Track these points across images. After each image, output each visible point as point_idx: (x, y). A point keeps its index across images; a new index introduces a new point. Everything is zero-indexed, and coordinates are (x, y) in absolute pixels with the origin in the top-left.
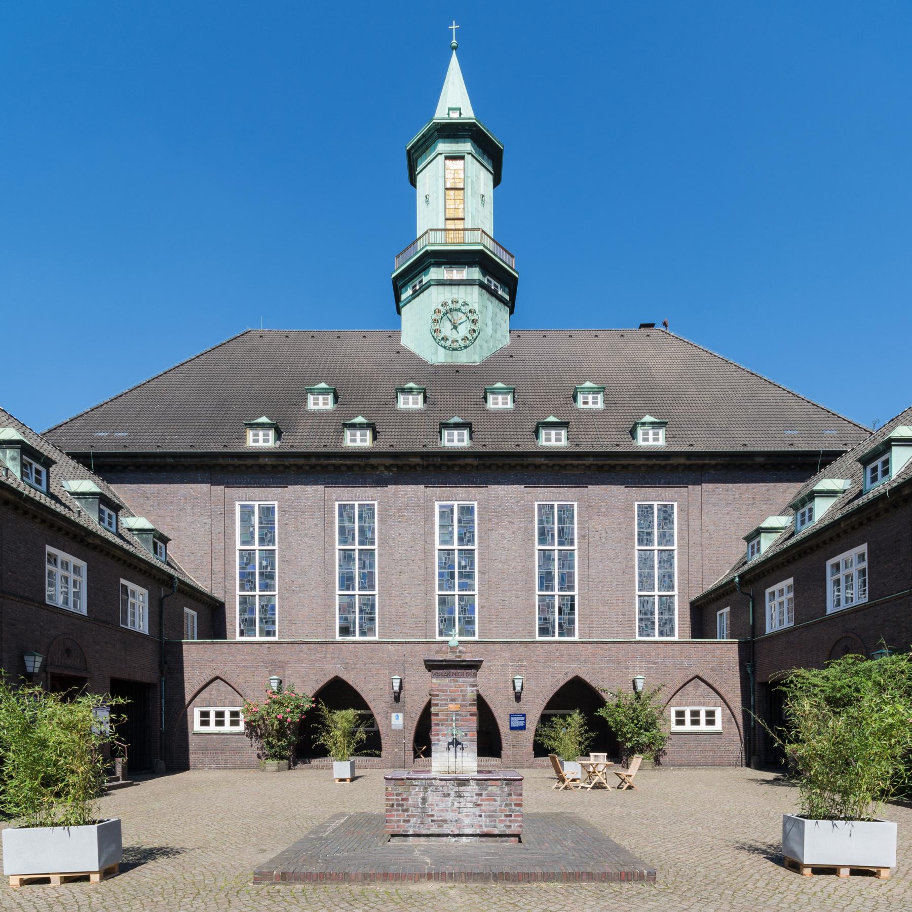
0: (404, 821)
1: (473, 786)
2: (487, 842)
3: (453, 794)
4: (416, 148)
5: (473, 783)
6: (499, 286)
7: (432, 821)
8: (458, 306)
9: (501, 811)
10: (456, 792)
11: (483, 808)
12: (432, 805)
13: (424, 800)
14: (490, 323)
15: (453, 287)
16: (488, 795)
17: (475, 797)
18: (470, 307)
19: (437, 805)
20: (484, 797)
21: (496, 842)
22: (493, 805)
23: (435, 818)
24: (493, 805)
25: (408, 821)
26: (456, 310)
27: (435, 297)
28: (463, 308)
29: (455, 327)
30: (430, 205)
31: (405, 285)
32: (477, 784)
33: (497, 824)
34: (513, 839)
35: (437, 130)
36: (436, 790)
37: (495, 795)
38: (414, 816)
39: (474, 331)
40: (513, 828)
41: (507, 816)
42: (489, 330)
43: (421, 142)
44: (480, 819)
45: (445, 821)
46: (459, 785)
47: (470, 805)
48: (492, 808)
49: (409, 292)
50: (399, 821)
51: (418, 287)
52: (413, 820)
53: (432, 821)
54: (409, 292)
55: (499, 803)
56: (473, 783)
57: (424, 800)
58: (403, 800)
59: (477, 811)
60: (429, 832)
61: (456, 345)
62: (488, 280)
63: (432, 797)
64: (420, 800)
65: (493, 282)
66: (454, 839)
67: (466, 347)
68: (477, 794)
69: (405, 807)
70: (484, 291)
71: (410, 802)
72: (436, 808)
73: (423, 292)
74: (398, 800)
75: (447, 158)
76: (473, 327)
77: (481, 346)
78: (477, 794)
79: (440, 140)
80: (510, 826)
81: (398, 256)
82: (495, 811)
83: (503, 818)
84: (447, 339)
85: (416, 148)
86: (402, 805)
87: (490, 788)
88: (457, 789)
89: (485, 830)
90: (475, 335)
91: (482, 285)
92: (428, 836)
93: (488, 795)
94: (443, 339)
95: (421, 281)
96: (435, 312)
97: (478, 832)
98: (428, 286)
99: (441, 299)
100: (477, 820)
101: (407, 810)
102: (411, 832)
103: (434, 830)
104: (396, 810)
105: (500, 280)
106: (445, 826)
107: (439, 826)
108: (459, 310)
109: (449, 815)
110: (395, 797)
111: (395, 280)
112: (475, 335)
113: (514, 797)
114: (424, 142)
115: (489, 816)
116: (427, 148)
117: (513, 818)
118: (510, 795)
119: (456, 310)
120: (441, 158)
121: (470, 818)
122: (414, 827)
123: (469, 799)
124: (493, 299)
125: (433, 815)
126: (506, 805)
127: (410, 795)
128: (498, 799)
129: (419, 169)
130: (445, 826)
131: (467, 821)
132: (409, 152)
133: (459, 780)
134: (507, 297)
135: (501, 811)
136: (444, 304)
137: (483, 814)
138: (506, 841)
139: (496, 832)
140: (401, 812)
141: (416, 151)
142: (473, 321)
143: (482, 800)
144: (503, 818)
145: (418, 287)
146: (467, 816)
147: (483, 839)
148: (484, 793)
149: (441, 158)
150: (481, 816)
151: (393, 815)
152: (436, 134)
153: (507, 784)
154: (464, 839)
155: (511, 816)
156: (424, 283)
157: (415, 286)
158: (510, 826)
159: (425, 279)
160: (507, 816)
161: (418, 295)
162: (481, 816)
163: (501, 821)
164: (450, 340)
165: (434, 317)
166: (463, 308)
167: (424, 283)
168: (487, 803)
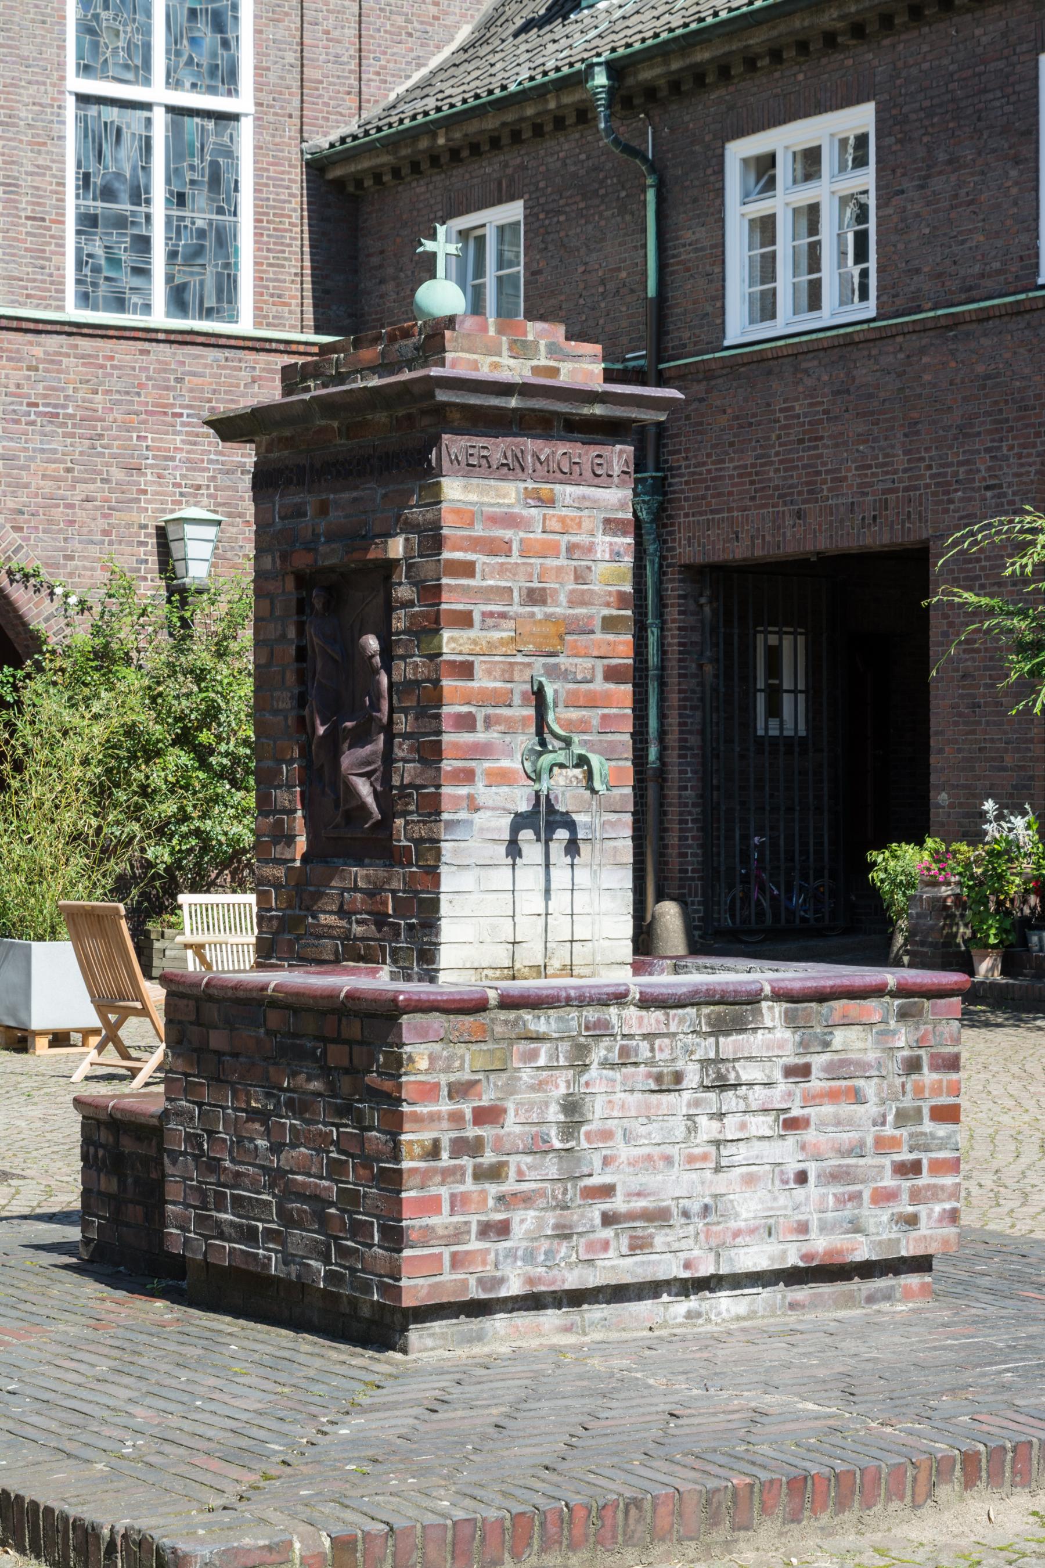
0: (486, 1230)
2: (814, 1304)
3: (692, 1076)
7: (608, 1219)
9: (883, 1145)
11: (810, 1135)
12: (607, 1135)
13: (572, 1107)
17: (783, 1086)
19: (628, 1136)
20: (816, 1083)
21: (849, 1301)
23: (618, 1204)
24: (849, 1123)
25: (503, 1229)
36: (626, 1059)
37: (861, 1069)
38: (526, 1200)
40: (924, 1228)
44: (800, 1193)
45: (659, 1216)
46: (720, 1029)
47: (761, 1125)
48: (847, 1137)
50: (458, 1235)
52: (524, 1222)
53: (608, 1219)
55: (871, 1109)
56: (772, 1013)
57: (572, 1107)
59: (786, 1152)
60: (592, 1279)
63: (609, 1095)
64: (555, 1114)
66: (681, 1307)
68: (790, 1071)
69: (489, 1158)
71: (512, 1125)
72: (624, 1152)
80: (912, 1221)
82: (857, 1150)
83: (889, 1182)
86: (475, 1147)
88: (706, 1048)
89: (821, 1245)
92: (576, 1298)
93: (834, 1072)
97: (793, 1260)
100: (788, 1203)
101: (494, 1173)
102: (514, 1288)
103: (618, 1267)
104: (447, 1174)
106: (660, 1240)
107: (639, 1245)
109: (675, 1186)
110: (445, 1106)
113: (928, 1076)
115: (835, 1177)
117: (925, 1179)
118: (913, 1066)
121: (762, 1193)
122: (530, 1257)
123: (758, 1096)
125: (608, 1191)
127: (510, 1089)
128: (870, 1088)
130: (660, 1240)
131: (748, 1207)
135: (883, 1145)
137: (812, 1169)
138: (888, 1296)
139: (863, 1252)
140: (469, 1185)
143: (810, 1099)
144: (889, 1182)
146: (750, 1180)
147: (801, 1293)
148: (818, 1061)
150: (802, 1178)
153: (903, 1015)
154: (726, 1304)
158: (912, 1221)
168: (828, 1109)
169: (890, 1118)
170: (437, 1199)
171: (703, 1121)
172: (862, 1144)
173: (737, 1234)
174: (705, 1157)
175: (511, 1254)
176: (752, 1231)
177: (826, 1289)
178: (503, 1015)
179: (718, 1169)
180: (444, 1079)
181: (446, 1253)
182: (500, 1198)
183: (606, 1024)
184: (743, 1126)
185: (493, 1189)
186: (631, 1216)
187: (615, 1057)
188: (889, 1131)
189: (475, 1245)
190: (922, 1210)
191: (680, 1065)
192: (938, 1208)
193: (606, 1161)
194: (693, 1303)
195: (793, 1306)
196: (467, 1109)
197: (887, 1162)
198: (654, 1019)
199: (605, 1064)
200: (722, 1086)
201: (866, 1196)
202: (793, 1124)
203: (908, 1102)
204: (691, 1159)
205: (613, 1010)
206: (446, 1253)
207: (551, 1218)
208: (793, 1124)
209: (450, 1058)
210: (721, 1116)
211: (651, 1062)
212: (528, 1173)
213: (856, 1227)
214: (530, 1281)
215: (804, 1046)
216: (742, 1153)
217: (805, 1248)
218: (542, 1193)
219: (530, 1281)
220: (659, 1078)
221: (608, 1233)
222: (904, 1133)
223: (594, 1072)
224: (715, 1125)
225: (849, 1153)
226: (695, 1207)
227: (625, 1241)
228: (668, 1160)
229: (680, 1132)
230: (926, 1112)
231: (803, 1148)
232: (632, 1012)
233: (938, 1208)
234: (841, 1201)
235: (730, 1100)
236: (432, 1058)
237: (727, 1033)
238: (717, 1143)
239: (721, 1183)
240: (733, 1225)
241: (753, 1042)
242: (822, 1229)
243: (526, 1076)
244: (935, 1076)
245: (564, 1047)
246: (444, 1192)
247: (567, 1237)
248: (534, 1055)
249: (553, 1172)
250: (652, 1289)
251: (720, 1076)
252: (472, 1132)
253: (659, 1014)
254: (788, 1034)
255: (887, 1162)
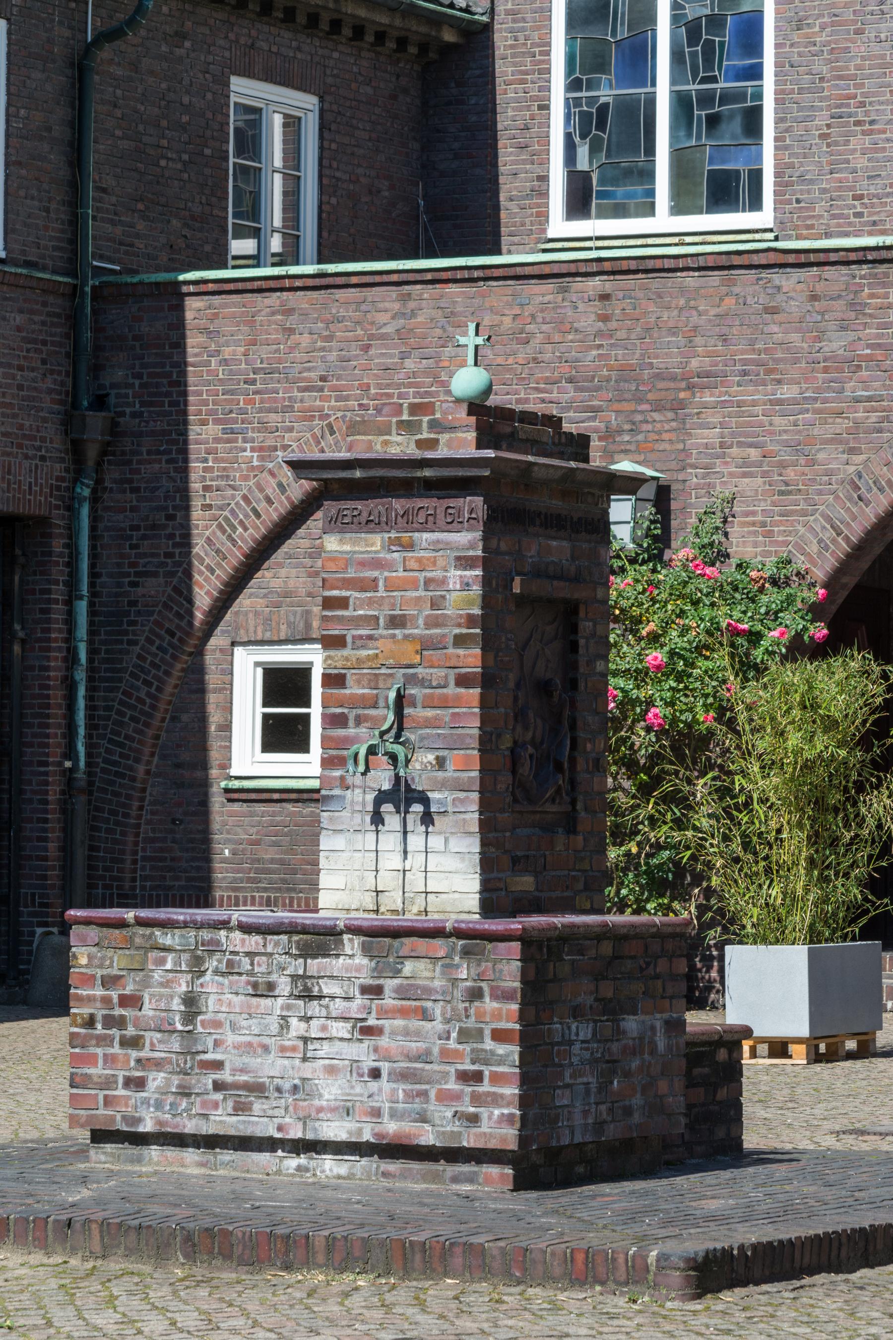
0: (129, 1082)
1: (352, 960)
2: (403, 1176)
3: (284, 986)
5: (352, 944)
7: (218, 1086)
10: (295, 978)
11: (384, 1042)
12: (218, 1024)
13: (191, 1001)
16: (403, 993)
17: (359, 1001)
19: (234, 1027)
20: (389, 1001)
21: (436, 1178)
22: (418, 1034)
23: (226, 1076)
24: (418, 1034)
25: (139, 1084)
32: (366, 950)
33: (433, 1107)
34: (494, 1170)
36: (231, 970)
38: (158, 1065)
40: (485, 1127)
41: (465, 1077)
44: (374, 1086)
45: (257, 1089)
46: (307, 952)
47: (340, 1029)
48: (415, 1046)
50: (108, 1083)
52: (156, 1080)
53: (218, 1086)
55: (438, 1026)
56: (352, 944)
57: (191, 1001)
58: (124, 1001)
59: (361, 1052)
63: (220, 996)
64: (177, 1005)
66: (293, 1162)
68: (365, 990)
69: (131, 1031)
71: (148, 1010)
72: (231, 1038)
74: (106, 1000)
78: (365, 990)
80: (474, 1119)
82: (424, 1057)
86: (121, 1023)
87: (408, 967)
88: (297, 966)
89: (391, 1127)
97: (367, 1136)
101: (134, 1043)
102: (147, 1126)
103: (223, 1120)
104: (103, 1041)
106: (258, 1106)
107: (241, 1108)
109: (271, 1067)
110: (99, 992)
115: (404, 1076)
117: (486, 1087)
118: (475, 995)
121: (342, 1081)
122: (159, 1105)
123: (338, 1006)
125: (218, 1065)
126: (465, 1035)
128: (437, 1010)
130: (258, 1106)
131: (331, 1091)
133: (304, 930)
135: (447, 1056)
137: (385, 1067)
139: (428, 1137)
140: (116, 1049)
143: (383, 1013)
144: (452, 1085)
146: (331, 1070)
147: (393, 1166)
148: (390, 984)
150: (375, 1074)
151: (91, 1060)
153: (466, 953)
154: (330, 1166)
155: (478, 1077)
158: (474, 1119)
160: (465, 1077)
162: (375, 1074)
163: (445, 1097)
168: (399, 1023)
169: (454, 1035)
170: (95, 1056)
171: (294, 1022)
172: (428, 1052)
173: (320, 1110)
174: (294, 1049)
175: (146, 1102)
176: (333, 1110)
177: (415, 1166)
178: (141, 931)
179: (305, 1059)
180: (99, 973)
181: (101, 1094)
182: (138, 1060)
183: (218, 943)
184: (324, 1028)
185: (134, 1054)
186: (236, 1086)
187: (223, 967)
188: (452, 1044)
189: (121, 1092)
190: (483, 1112)
191: (274, 977)
192: (497, 1112)
193: (217, 1043)
194: (303, 1160)
195: (385, 1174)
196: (114, 995)
197: (452, 1069)
198: (254, 942)
199: (216, 972)
200: (308, 996)
201: (432, 1094)
202: (368, 1031)
203: (471, 1023)
204: (283, 1049)
205: (223, 933)
206: (101, 1094)
207: (176, 1080)
208: (368, 1031)
209: (103, 958)
210: (307, 1019)
211: (251, 973)
212: (157, 1046)
213: (423, 1118)
214: (160, 1123)
215: (378, 972)
216: (326, 1049)
217: (378, 1129)
218: (170, 1062)
219: (160, 1123)
220: (255, 985)
221: (219, 1096)
222: (467, 1048)
223: (208, 977)
224: (303, 1025)
225: (418, 1058)
226: (287, 1086)
227: (230, 1104)
228: (266, 1049)
229: (274, 1028)
230: (487, 1033)
231: (376, 1050)
232: (237, 935)
233: (497, 1112)
234: (410, 1096)
235: (314, 1008)
236: (90, 957)
237: (314, 956)
238: (306, 1040)
239: (307, 1070)
240: (317, 1102)
241: (337, 965)
242: (394, 1114)
243: (157, 976)
244: (495, 1005)
245: (185, 957)
246: (99, 1051)
247: (188, 1095)
248: (163, 961)
249: (176, 1047)
250: (269, 1144)
251: (307, 989)
252: (118, 1012)
253: (258, 938)
254: (365, 961)
255: (452, 1069)
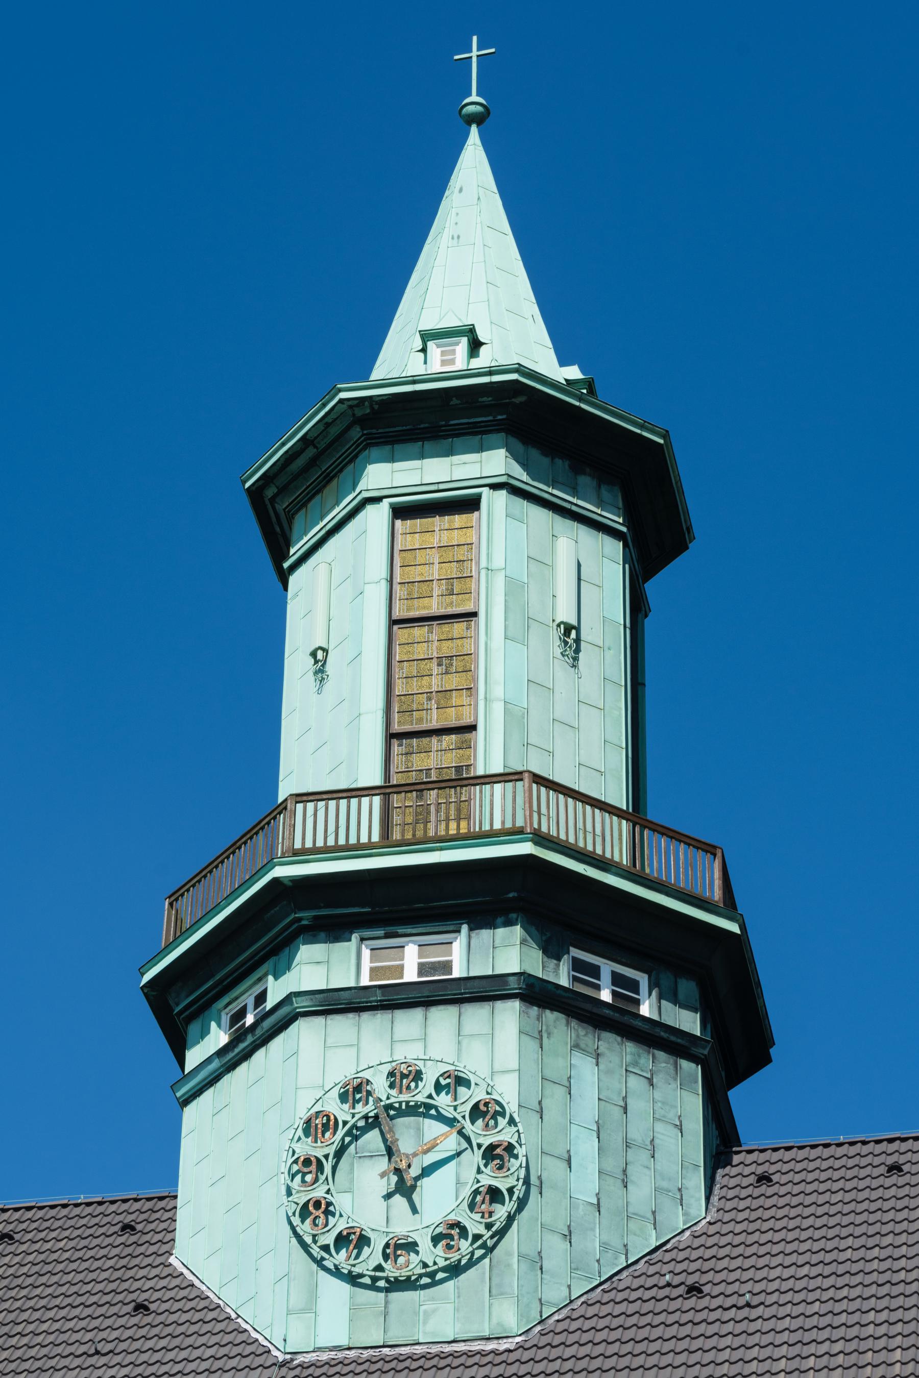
4: (282, 480)
6: (643, 980)
8: (423, 1092)
14: (586, 1148)
15: (399, 1014)
18: (479, 1095)
26: (412, 1110)
27: (312, 1065)
28: (443, 1101)
29: (405, 1188)
30: (329, 686)
31: (201, 1010)
35: (361, 421)
39: (495, 1195)
42: (585, 1182)
43: (300, 462)
49: (218, 1037)
51: (250, 1020)
54: (218, 1037)
61: (409, 1266)
62: (578, 965)
65: (607, 967)
67: (455, 1270)
70: (550, 1016)
73: (265, 1041)
75: (400, 512)
76: (486, 1180)
77: (537, 1262)
79: (375, 452)
81: (175, 896)
84: (363, 1241)
85: (282, 480)
90: (501, 1212)
91: (535, 994)
94: (342, 1240)
95: (261, 998)
96: (308, 1127)
98: (281, 1020)
99: (343, 1069)
105: (643, 955)
108: (424, 1110)
111: (159, 994)
112: (501, 1212)
114: (313, 462)
116: (328, 478)
119: (412, 1110)
120: (377, 518)
124: (609, 1042)
129: (296, 550)
132: (256, 495)
134: (689, 1022)
136: (354, 1091)
141: (282, 490)
142: (490, 1153)
145: (250, 1020)
149: (377, 518)
152: (356, 433)
156: (269, 1004)
157: (241, 1014)
159: (276, 990)
161: (247, 1055)
164: (378, 1243)
165: (306, 1148)
166: (443, 1101)
167: (269, 1004)
